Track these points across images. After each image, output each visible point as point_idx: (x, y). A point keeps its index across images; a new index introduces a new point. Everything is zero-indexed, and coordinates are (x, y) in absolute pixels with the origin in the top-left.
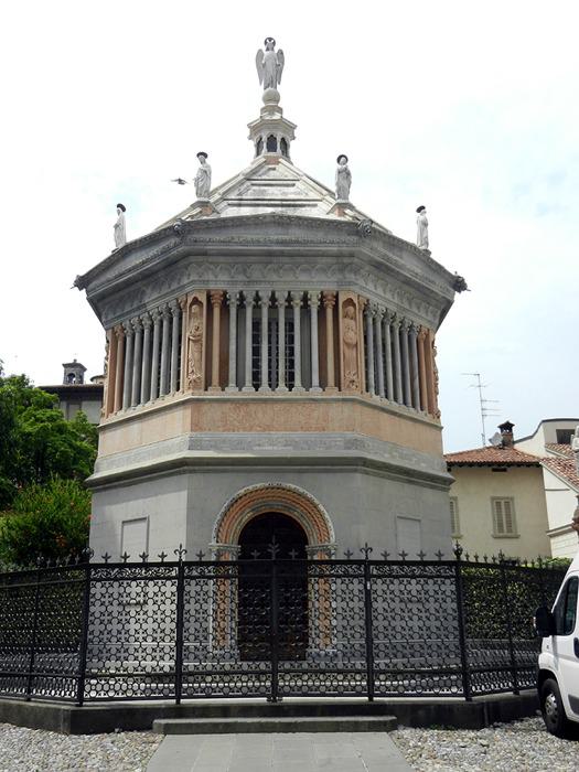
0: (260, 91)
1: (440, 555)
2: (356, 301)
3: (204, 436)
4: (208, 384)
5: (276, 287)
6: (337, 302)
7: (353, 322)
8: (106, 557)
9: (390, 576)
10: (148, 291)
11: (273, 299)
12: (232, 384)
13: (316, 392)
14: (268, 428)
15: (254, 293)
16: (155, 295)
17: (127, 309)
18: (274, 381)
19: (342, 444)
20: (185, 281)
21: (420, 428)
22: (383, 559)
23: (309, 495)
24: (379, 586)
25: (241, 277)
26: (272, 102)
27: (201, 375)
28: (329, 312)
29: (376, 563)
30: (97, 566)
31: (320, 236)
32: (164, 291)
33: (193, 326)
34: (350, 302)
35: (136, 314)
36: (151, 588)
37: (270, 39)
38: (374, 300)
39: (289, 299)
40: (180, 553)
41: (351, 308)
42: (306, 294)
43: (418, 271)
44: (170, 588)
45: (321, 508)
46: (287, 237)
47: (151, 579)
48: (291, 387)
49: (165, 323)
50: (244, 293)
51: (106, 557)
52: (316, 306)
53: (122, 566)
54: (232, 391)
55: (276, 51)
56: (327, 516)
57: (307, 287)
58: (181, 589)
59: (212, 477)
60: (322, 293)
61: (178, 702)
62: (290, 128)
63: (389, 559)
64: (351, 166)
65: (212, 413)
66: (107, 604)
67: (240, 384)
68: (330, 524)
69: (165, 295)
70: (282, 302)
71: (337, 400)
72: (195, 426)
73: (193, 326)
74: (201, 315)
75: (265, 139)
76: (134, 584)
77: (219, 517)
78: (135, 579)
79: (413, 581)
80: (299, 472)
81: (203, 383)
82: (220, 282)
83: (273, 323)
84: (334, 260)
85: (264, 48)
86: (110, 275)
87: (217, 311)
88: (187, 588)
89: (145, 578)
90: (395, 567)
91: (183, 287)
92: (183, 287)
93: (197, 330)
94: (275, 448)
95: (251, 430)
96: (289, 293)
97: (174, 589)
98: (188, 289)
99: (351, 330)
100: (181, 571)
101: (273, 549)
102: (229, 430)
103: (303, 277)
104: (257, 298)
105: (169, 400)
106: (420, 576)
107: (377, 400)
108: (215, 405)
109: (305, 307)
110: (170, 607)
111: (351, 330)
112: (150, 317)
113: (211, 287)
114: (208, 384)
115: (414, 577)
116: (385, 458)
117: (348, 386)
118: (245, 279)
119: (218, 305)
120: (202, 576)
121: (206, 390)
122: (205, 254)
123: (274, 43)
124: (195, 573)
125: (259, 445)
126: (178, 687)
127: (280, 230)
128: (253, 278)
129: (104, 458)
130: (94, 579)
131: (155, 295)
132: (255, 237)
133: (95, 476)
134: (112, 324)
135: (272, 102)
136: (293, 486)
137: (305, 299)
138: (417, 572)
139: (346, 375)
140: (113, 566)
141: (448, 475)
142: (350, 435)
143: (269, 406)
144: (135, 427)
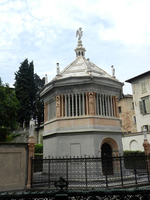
3: (96, 126)
10: (75, 89)
14: (106, 125)
37: (81, 28)
45: (117, 143)
46: (110, 83)
62: (84, 50)
64: (114, 67)
65: (96, 120)
69: (81, 91)
71: (117, 120)
72: (94, 123)
80: (112, 135)
82: (96, 90)
84: (115, 89)
85: (79, 30)
86: (64, 82)
95: (103, 125)
98: (88, 91)
100: (120, 159)
108: (97, 119)
113: (94, 91)
118: (100, 91)
122: (94, 84)
127: (108, 82)
128: (102, 91)
132: (105, 82)
134: (60, 94)
136: (112, 138)
144: (72, 121)
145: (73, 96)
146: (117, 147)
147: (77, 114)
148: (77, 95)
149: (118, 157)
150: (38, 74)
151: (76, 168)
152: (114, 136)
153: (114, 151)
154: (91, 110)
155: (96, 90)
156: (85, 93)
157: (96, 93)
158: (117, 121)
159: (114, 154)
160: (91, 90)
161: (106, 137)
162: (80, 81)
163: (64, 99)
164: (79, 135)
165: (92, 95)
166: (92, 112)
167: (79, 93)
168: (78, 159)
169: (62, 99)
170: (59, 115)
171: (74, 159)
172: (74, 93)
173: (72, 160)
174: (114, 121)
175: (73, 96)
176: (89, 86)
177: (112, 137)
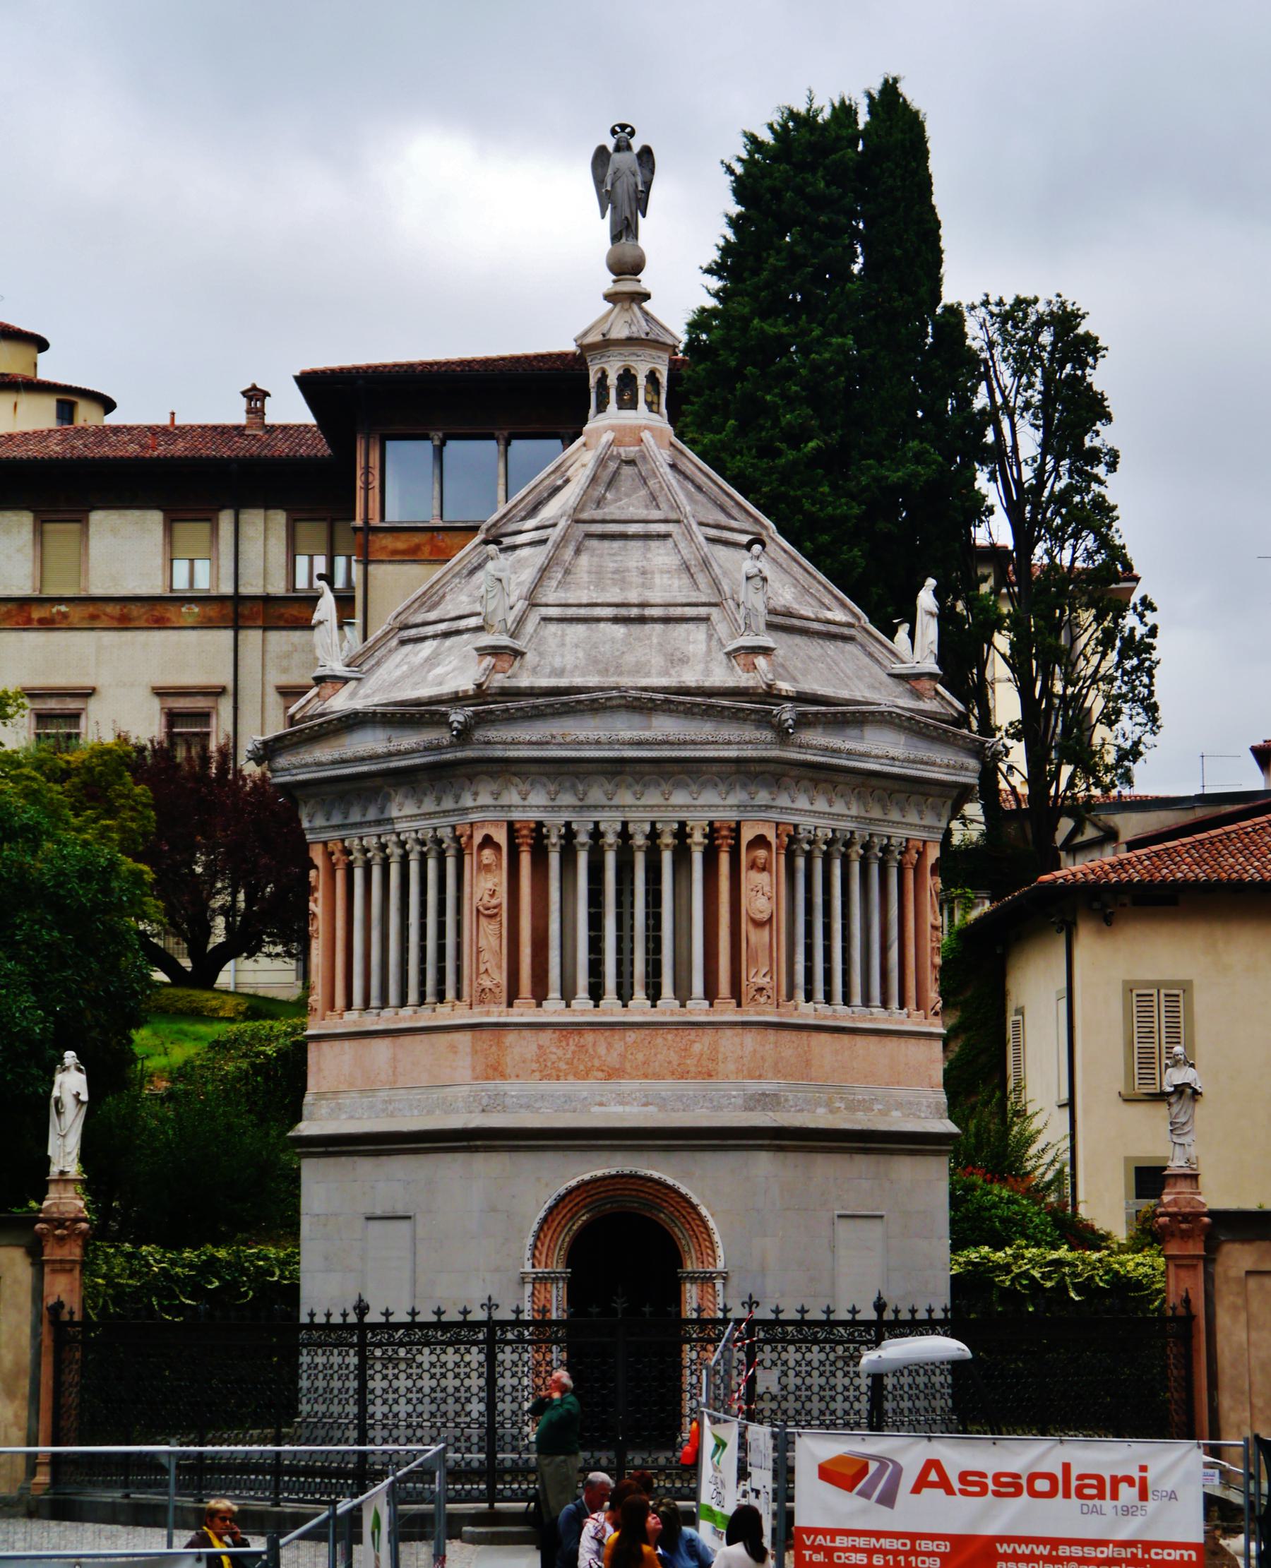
0: (604, 227)
1: (854, 1311)
2: (771, 837)
3: (512, 1088)
4: (513, 995)
5: (630, 815)
6: (737, 838)
7: (765, 875)
8: (387, 1314)
9: (782, 1340)
11: (625, 834)
12: (554, 994)
13: (698, 1009)
14: (612, 1074)
15: (591, 826)
16: (410, 809)
17: (355, 817)
18: (626, 990)
19: (740, 1101)
20: (468, 801)
21: (892, 1044)
22: (772, 1316)
23: (684, 1190)
24: (766, 1354)
25: (567, 799)
26: (627, 266)
27: (503, 979)
28: (724, 859)
29: (764, 1323)
30: (374, 1327)
31: (703, 729)
32: (429, 805)
33: (487, 885)
34: (760, 841)
35: (375, 830)
36: (450, 1357)
38: (806, 822)
39: (654, 835)
40: (490, 1308)
41: (761, 853)
42: (682, 824)
44: (475, 1356)
45: (704, 1211)
47: (450, 1343)
48: (654, 994)
49: (432, 864)
50: (574, 826)
51: (387, 1314)
52: (701, 848)
54: (553, 1010)
55: (636, 148)
56: (711, 1224)
57: (683, 815)
58: (491, 1358)
60: (711, 824)
61: (491, 1507)
63: (782, 1317)
65: (521, 1047)
66: (390, 1377)
67: (568, 995)
68: (717, 1238)
73: (487, 885)
74: (499, 866)
75: (612, 381)
76: (426, 1351)
77: (535, 1227)
78: (427, 1344)
79: (815, 1348)
81: (504, 995)
82: (532, 804)
85: (610, 143)
87: (525, 860)
88: (500, 1357)
89: (442, 1343)
90: (790, 1329)
91: (465, 811)
92: (465, 811)
93: (492, 896)
94: (628, 1109)
95: (586, 1076)
96: (653, 824)
97: (482, 1357)
98: (474, 817)
99: (761, 892)
100: (491, 1333)
101: (619, 1304)
102: (548, 1077)
103: (680, 798)
104: (597, 834)
105: (445, 1014)
106: (826, 1341)
107: (806, 1012)
108: (527, 1033)
110: (476, 1382)
111: (761, 892)
112: (402, 844)
113: (516, 815)
114: (513, 995)
115: (816, 1341)
116: (820, 1119)
117: (753, 999)
119: (529, 843)
120: (520, 1340)
121: (510, 1005)
123: (632, 134)
124: (510, 1336)
125: (601, 1104)
126: (491, 1487)
127: (637, 719)
128: (590, 801)
129: (321, 1095)
130: (372, 1344)
132: (593, 735)
133: (306, 1128)
134: (324, 836)
135: (627, 266)
137: (682, 833)
138: (821, 1336)
139: (755, 977)
140: (398, 1326)
142: (754, 1086)
143: (617, 1035)
144: (382, 1048)
145: (394, 851)
147: (413, 997)
148: (418, 848)
149: (477, 1325)
151: (403, 1383)
154: (482, 969)
155: (532, 804)
156: (454, 828)
157: (540, 824)
158: (729, 1033)
160: (483, 808)
161: (599, 1173)
162: (409, 740)
164: (461, 1157)
165: (497, 847)
166: (486, 982)
169: (340, 875)
172: (399, 826)
174: (701, 1043)
175: (394, 851)
176: (471, 778)
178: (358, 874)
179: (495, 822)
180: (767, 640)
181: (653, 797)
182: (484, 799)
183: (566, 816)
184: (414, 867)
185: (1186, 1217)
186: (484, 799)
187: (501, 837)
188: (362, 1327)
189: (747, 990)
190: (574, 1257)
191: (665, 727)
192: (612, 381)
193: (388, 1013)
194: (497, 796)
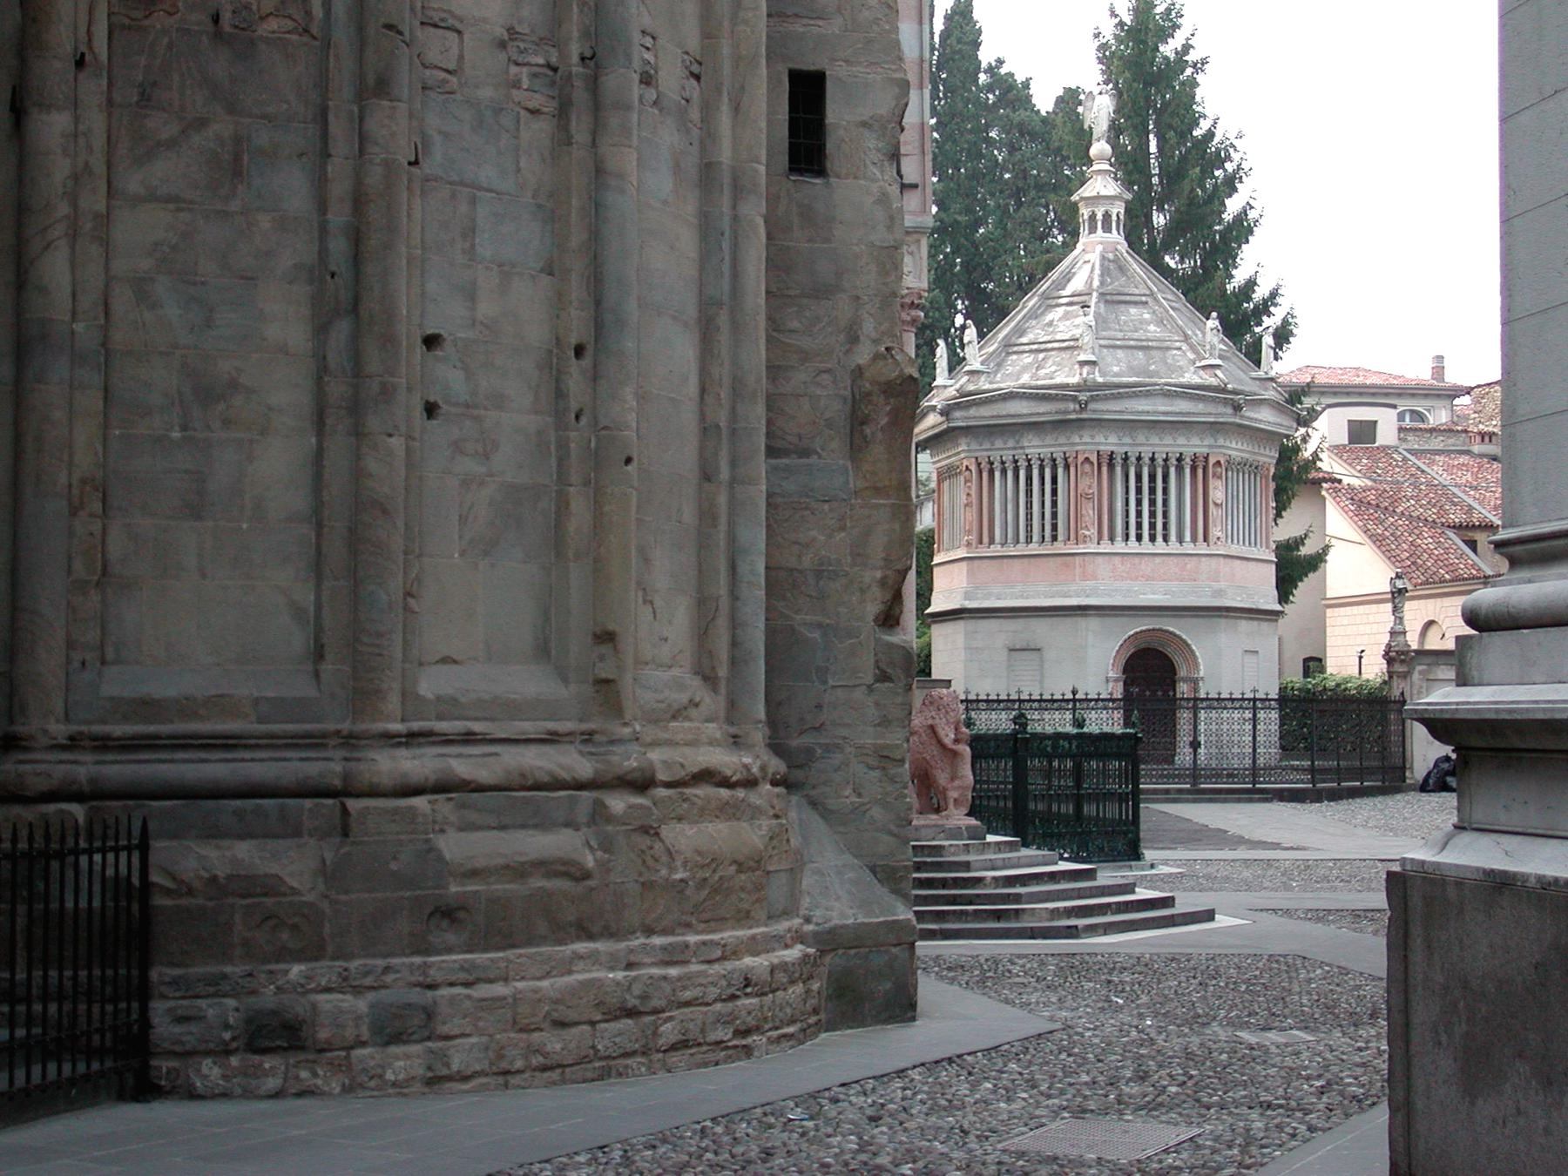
25: (1127, 440)
28: (1200, 471)
31: (1201, 407)
34: (1218, 463)
38: (1233, 453)
43: (1271, 419)
48: (1166, 539)
53: (1097, 700)
59: (1109, 621)
70: (1160, 461)
75: (1099, 217)
82: (1110, 442)
83: (1152, 478)
91: (1074, 444)
92: (1074, 444)
103: (1181, 441)
105: (1059, 547)
109: (1180, 469)
113: (1102, 448)
127: (1166, 400)
131: (1035, 443)
139: (1215, 532)
141: (1278, 607)
142: (1216, 585)
145: (1022, 464)
146: (1196, 665)
150: (1017, 68)
152: (1183, 621)
153: (1185, 680)
159: (1183, 689)
162: (1043, 407)
163: (991, 472)
167: (1045, 452)
168: (999, 701)
169: (985, 475)
170: (973, 538)
171: (987, 701)
173: (982, 705)
174: (1191, 564)
175: (1022, 464)
177: (1171, 626)
178: (997, 474)
179: (1091, 452)
180: (1219, 362)
181: (1168, 440)
182: (1087, 439)
183: (1125, 449)
184: (1035, 473)
185: (1403, 653)
186: (1087, 439)
187: (1094, 459)
188: (1074, 700)
189: (1212, 539)
190: (1124, 672)
191: (1183, 406)
192: (1099, 217)
193: (1021, 546)
194: (1092, 437)
